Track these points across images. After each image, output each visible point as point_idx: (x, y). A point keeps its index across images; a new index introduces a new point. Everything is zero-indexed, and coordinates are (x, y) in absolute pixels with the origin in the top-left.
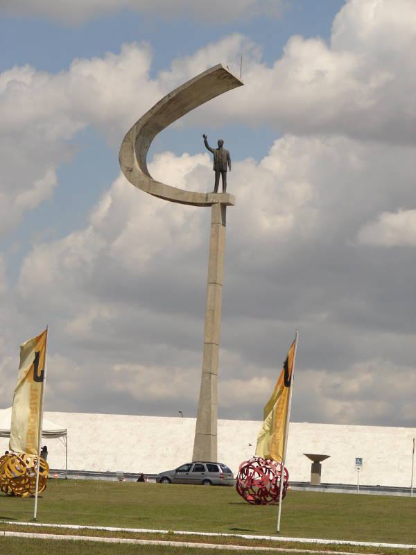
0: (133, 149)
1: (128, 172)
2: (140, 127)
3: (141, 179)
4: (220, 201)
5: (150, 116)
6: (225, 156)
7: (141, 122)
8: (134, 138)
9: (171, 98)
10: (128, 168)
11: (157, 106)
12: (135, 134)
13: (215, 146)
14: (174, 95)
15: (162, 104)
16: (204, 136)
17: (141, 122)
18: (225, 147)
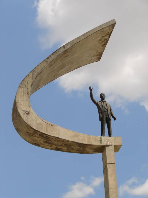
0: (28, 94)
1: (26, 115)
2: (35, 74)
3: (38, 122)
4: (114, 144)
5: (46, 64)
6: (109, 108)
7: (36, 70)
8: (30, 84)
9: (65, 49)
10: (25, 111)
11: (53, 56)
12: (31, 81)
13: (98, 99)
14: (69, 47)
15: (55, 55)
16: (91, 90)
17: (36, 70)
18: (106, 99)
